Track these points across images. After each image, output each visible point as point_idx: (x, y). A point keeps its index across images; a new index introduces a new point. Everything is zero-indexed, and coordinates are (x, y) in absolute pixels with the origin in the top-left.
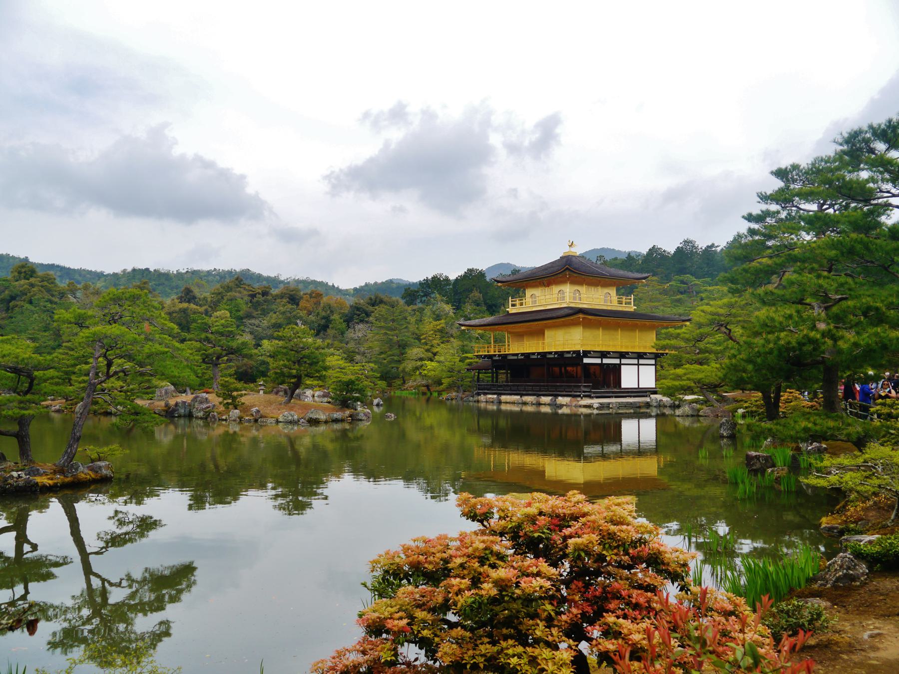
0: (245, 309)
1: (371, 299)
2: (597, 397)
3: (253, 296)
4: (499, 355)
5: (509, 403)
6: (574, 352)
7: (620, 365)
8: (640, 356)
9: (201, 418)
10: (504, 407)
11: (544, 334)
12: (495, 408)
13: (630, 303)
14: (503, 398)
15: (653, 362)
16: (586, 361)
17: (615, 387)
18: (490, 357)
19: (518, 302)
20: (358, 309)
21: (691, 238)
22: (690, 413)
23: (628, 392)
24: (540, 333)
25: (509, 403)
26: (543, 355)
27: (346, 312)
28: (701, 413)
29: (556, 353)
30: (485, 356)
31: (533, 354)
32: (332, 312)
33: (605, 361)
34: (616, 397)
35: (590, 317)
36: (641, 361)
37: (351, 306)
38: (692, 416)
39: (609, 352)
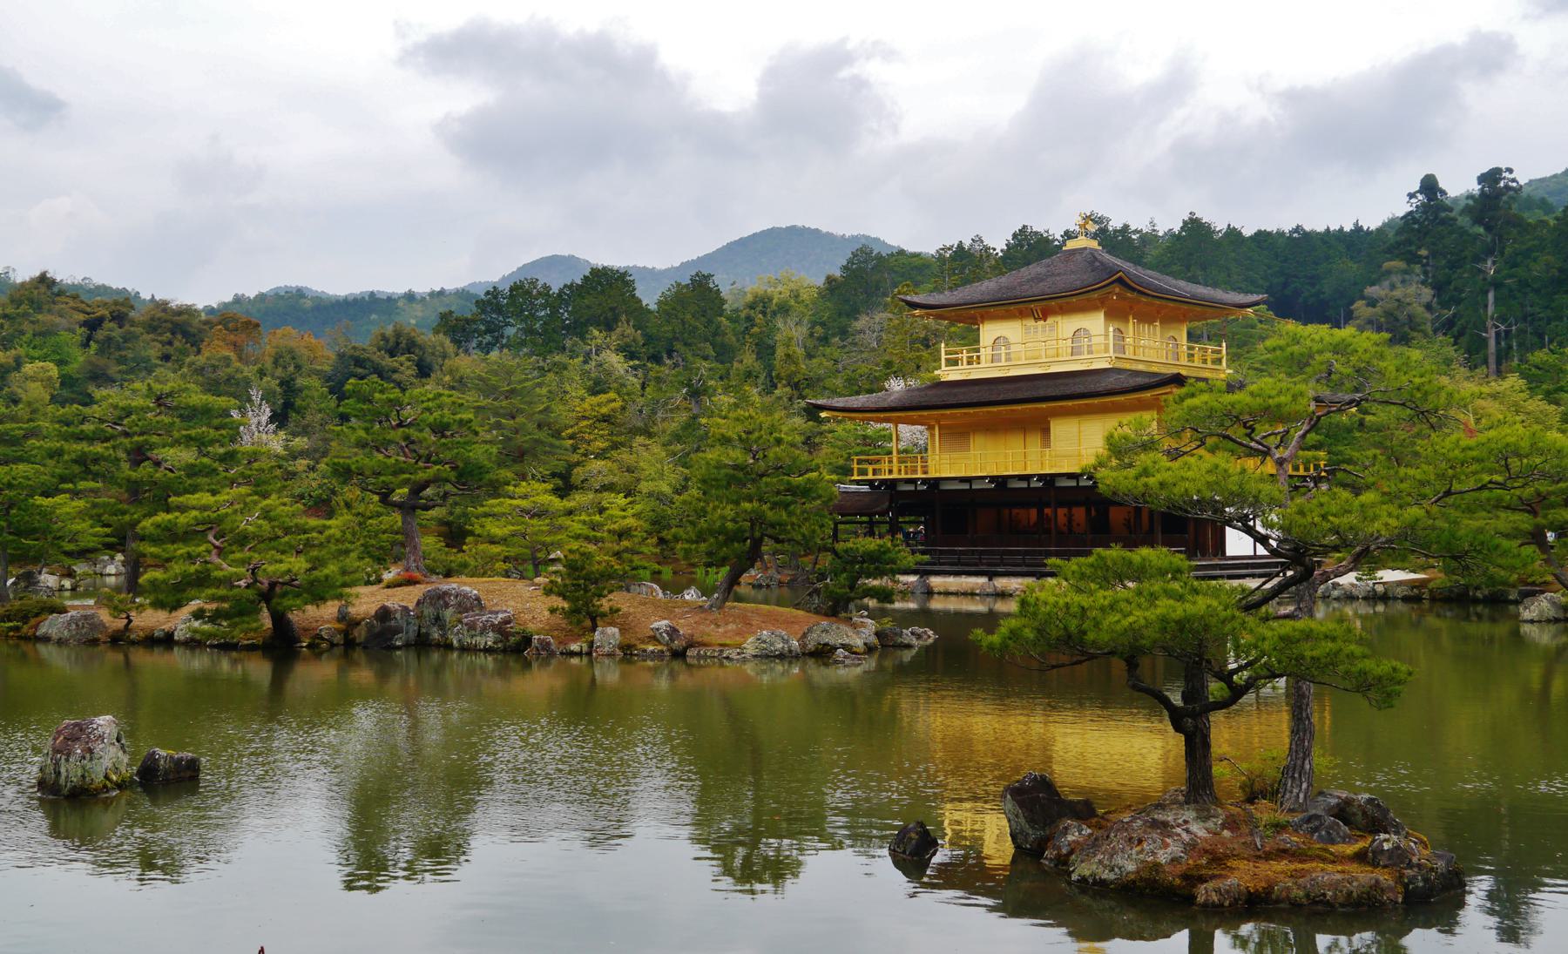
0: (79, 360)
1: (384, 338)
3: (93, 325)
4: (924, 481)
5: (956, 594)
9: (488, 651)
10: (936, 604)
11: (1046, 431)
12: (912, 606)
13: (1219, 361)
14: (935, 581)
17: (1215, 555)
18: (891, 484)
19: (965, 355)
20: (359, 362)
21: (1101, 212)
22: (1552, 613)
23: (1247, 566)
25: (956, 594)
26: (1049, 479)
27: (327, 368)
30: (883, 482)
31: (1027, 478)
32: (298, 367)
34: (1231, 577)
37: (341, 356)
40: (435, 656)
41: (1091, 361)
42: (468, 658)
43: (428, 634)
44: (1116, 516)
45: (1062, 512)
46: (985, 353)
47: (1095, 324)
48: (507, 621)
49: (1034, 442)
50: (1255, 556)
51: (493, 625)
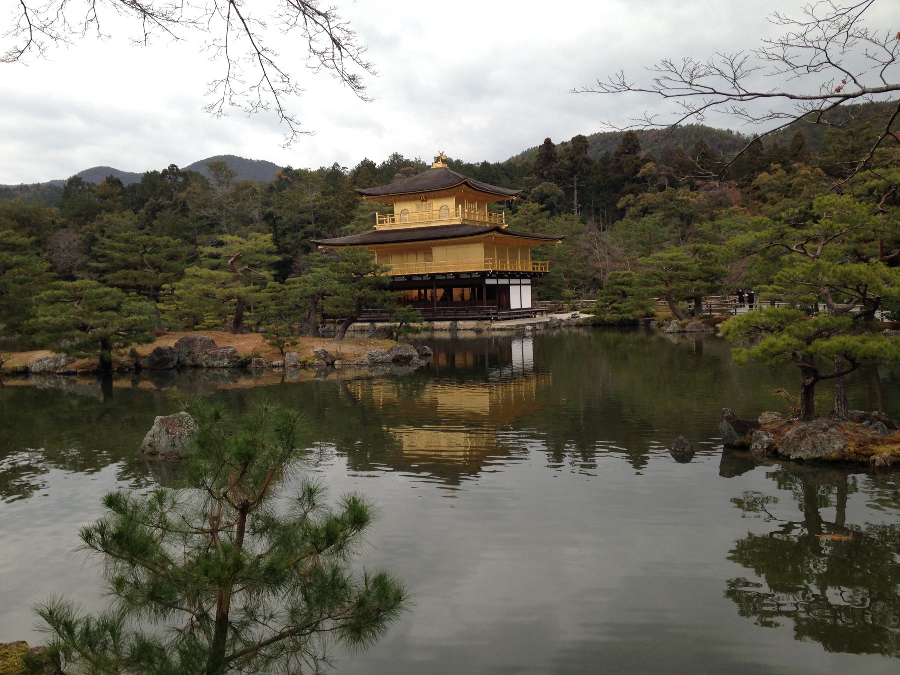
2: (504, 320)
6: (480, 273)
7: (509, 285)
8: (523, 276)
15: (529, 282)
16: (489, 282)
23: (521, 313)
24: (428, 253)
26: (433, 276)
28: (687, 328)
29: (454, 274)
33: (503, 282)
35: (501, 235)
36: (524, 281)
38: (680, 332)
39: (507, 273)
40: (190, 372)
41: (451, 221)
42: (211, 371)
43: (184, 361)
44: (457, 292)
45: (429, 292)
46: (397, 217)
47: (451, 203)
48: (235, 352)
49: (422, 257)
50: (522, 309)
51: (227, 354)
